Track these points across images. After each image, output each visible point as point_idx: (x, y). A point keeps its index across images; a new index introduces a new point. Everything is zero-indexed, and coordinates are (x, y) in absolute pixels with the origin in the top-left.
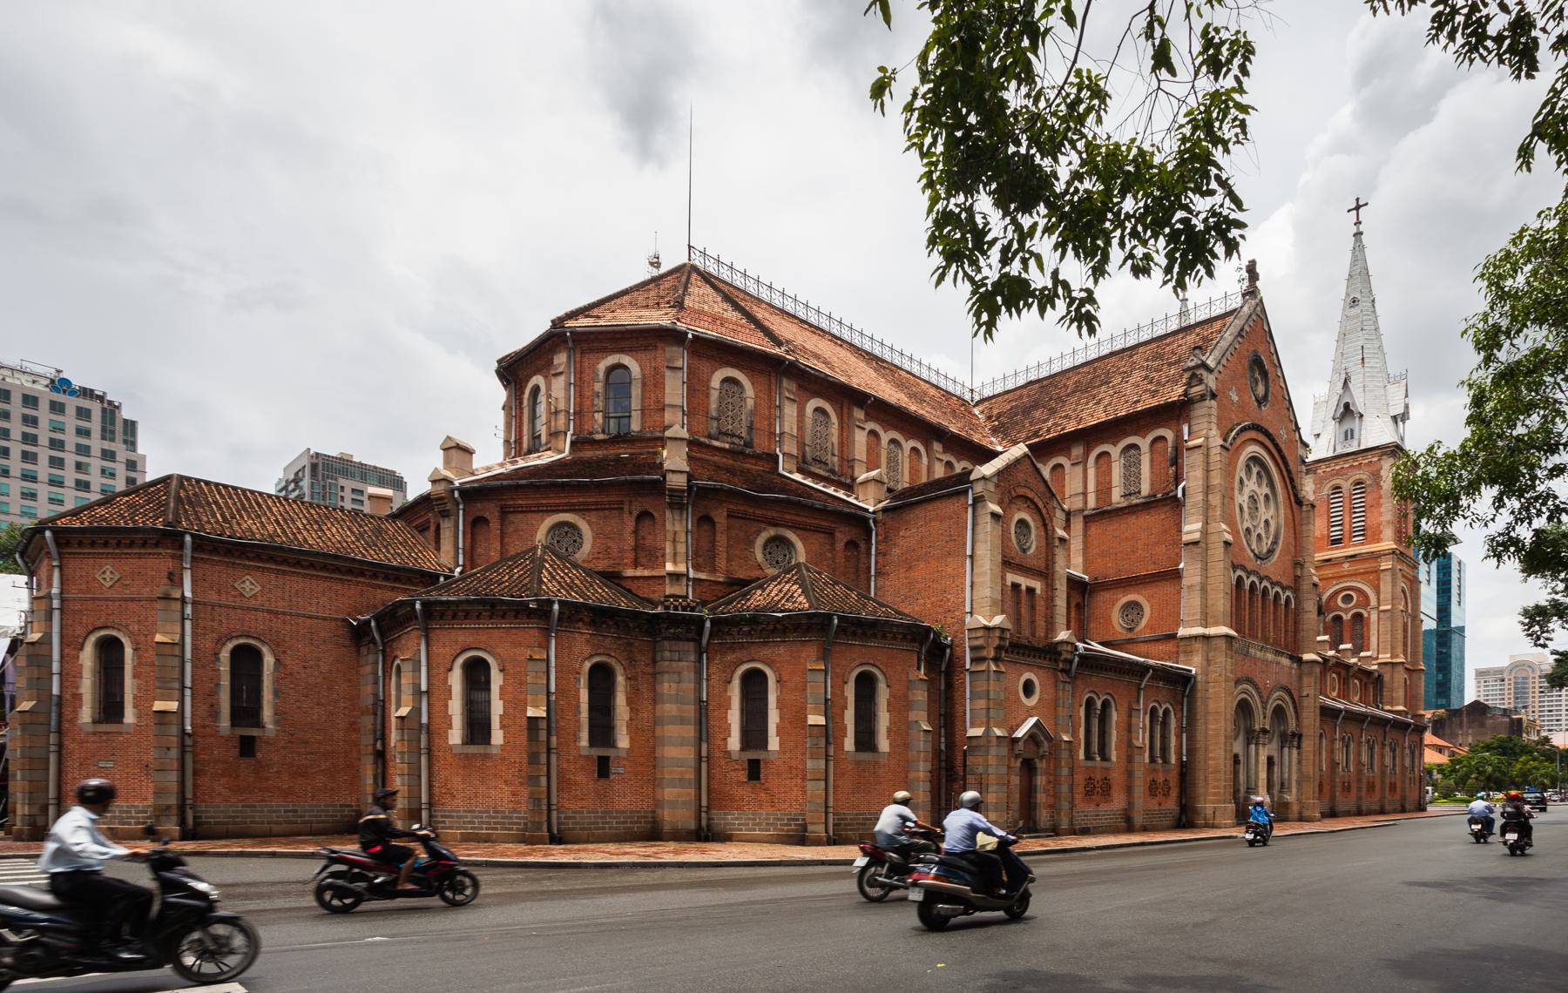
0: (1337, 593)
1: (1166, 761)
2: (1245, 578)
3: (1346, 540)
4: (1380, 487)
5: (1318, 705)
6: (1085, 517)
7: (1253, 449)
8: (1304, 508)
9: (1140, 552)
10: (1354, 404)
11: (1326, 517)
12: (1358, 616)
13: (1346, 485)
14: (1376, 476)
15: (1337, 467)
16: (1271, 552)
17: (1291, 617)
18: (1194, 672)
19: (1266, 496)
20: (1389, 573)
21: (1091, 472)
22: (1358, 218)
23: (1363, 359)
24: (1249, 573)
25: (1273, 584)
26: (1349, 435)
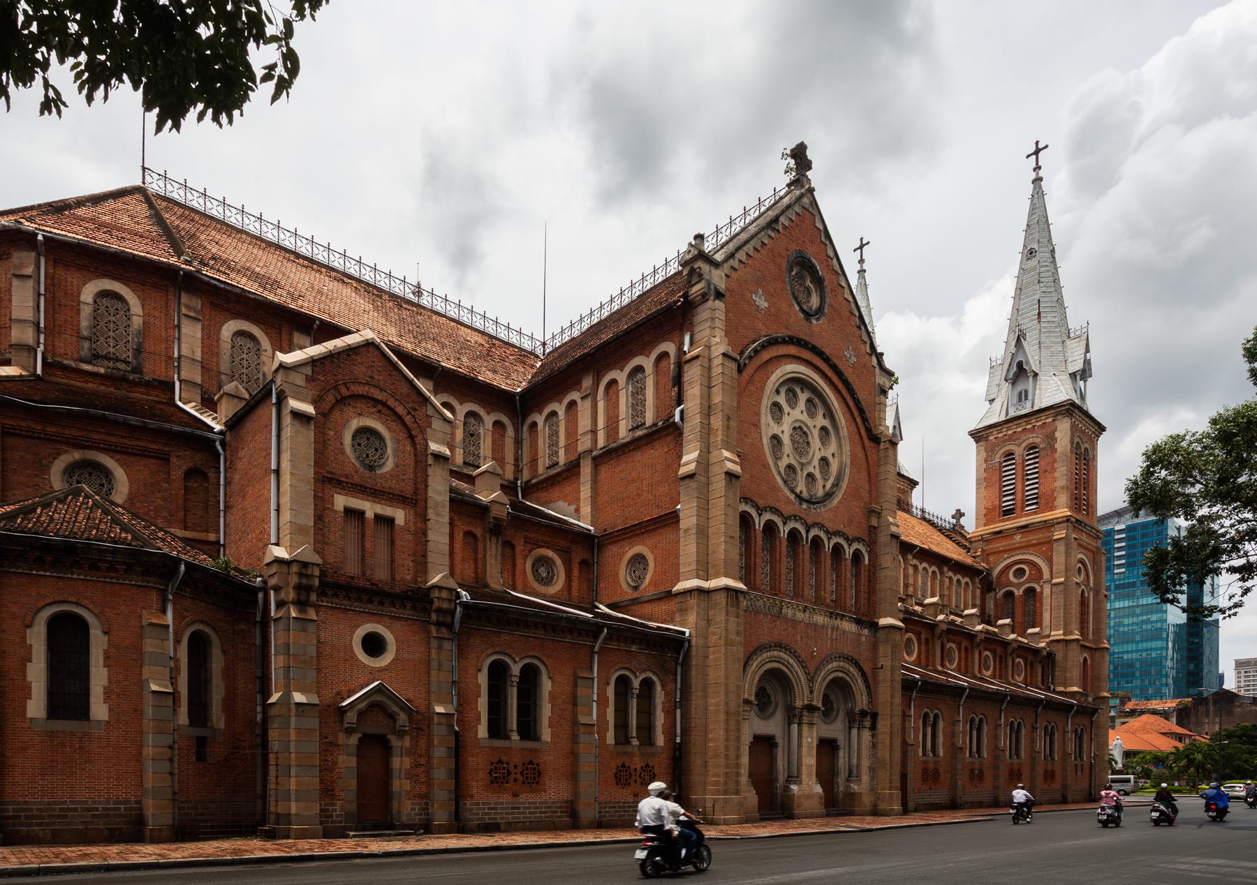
0: (1008, 567)
3: (1018, 510)
5: (898, 678)
6: (594, 459)
9: (645, 494)
10: (1028, 363)
11: (998, 486)
12: (1030, 591)
15: (1010, 432)
16: (829, 495)
17: (864, 574)
20: (1062, 543)
21: (601, 405)
24: (760, 512)
25: (831, 534)
26: (1023, 396)
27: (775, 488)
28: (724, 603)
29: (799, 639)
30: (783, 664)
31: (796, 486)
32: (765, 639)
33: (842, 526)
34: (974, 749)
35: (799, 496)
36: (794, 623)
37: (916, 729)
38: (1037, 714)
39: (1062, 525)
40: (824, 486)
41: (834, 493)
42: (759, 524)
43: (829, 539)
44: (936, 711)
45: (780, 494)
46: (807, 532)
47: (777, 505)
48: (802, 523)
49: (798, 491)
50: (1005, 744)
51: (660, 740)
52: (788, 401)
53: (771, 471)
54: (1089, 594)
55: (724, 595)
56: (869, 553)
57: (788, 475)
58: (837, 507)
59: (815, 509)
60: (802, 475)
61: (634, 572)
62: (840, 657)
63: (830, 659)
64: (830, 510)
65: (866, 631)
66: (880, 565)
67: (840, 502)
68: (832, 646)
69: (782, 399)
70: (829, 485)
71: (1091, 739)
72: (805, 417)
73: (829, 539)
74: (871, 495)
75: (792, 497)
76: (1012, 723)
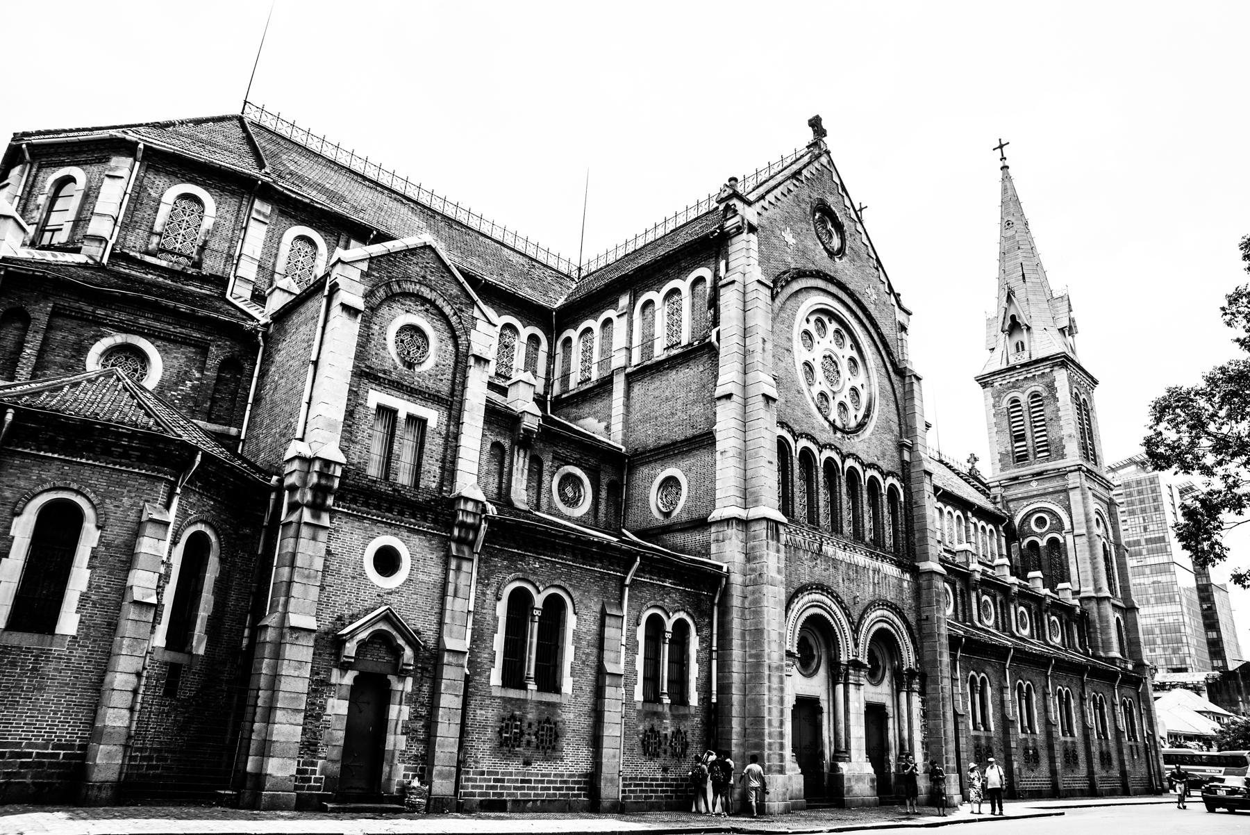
1: (680, 697)
2: (816, 452)
4: (1056, 400)
7: (817, 300)
13: (1024, 398)
14: (1051, 387)
16: (861, 426)
17: (900, 514)
19: (852, 359)
20: (1078, 492)
23: (1023, 275)
24: (796, 436)
26: (1020, 347)
27: (809, 415)
28: (765, 535)
29: (841, 581)
30: (825, 610)
32: (806, 579)
33: (876, 458)
35: (832, 424)
36: (835, 562)
39: (1074, 473)
40: (856, 416)
41: (866, 423)
45: (814, 421)
46: (843, 462)
48: (837, 453)
49: (831, 419)
51: (694, 699)
55: (764, 524)
57: (821, 402)
58: (870, 439)
61: (666, 496)
63: (872, 605)
67: (872, 434)
68: (874, 591)
70: (860, 415)
72: (834, 347)
73: (864, 471)
74: (900, 428)
75: (826, 424)
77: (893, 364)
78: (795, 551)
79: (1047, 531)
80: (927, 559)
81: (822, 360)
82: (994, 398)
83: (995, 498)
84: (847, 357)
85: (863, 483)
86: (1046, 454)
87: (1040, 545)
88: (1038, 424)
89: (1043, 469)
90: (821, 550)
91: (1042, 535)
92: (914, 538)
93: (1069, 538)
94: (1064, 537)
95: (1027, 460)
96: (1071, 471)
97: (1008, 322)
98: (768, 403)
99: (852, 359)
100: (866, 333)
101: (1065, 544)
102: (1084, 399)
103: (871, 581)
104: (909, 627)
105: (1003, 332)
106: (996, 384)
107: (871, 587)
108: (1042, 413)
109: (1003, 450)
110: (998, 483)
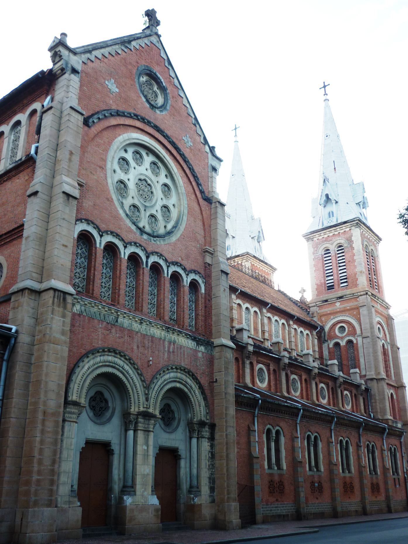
4: (353, 248)
8: (213, 205)
13: (333, 248)
14: (350, 240)
16: (169, 233)
17: (201, 301)
18: (13, 331)
22: (325, 92)
23: (335, 168)
25: (169, 264)
28: (51, 302)
29: (135, 347)
30: (118, 370)
31: (140, 221)
32: (99, 344)
33: (180, 259)
34: (313, 463)
35: (142, 231)
36: (131, 333)
37: (260, 443)
38: (359, 435)
39: (363, 297)
40: (165, 227)
42: (100, 243)
43: (168, 267)
44: (278, 428)
45: (121, 223)
46: (148, 257)
47: (118, 231)
48: (142, 250)
50: (337, 459)
52: (135, 160)
53: (114, 204)
54: (387, 347)
56: (205, 284)
57: (133, 212)
58: (175, 243)
59: (155, 241)
60: (145, 215)
62: (177, 369)
63: (168, 369)
64: (169, 244)
65: (202, 348)
66: (214, 295)
67: (178, 240)
68: (169, 358)
69: (129, 156)
71: (402, 457)
72: (149, 173)
74: (205, 240)
75: (133, 228)
76: (341, 441)
77: (202, 192)
78: (89, 321)
79: (345, 336)
80: (219, 337)
81: (137, 181)
82: (314, 248)
83: (313, 314)
84: (161, 183)
85: (166, 275)
86: (345, 284)
87: (341, 345)
88: (341, 265)
89: (343, 294)
90: (117, 321)
91: (342, 338)
92: (211, 321)
93: (360, 339)
94: (357, 339)
95: (334, 288)
96: (361, 295)
97: (324, 198)
98: (68, 199)
99: (166, 185)
100: (179, 167)
101: (357, 344)
102: (372, 249)
103: (166, 349)
104: (201, 387)
105: (320, 205)
106: (315, 239)
107: (166, 354)
108: (343, 257)
109: (317, 283)
110: (315, 304)
